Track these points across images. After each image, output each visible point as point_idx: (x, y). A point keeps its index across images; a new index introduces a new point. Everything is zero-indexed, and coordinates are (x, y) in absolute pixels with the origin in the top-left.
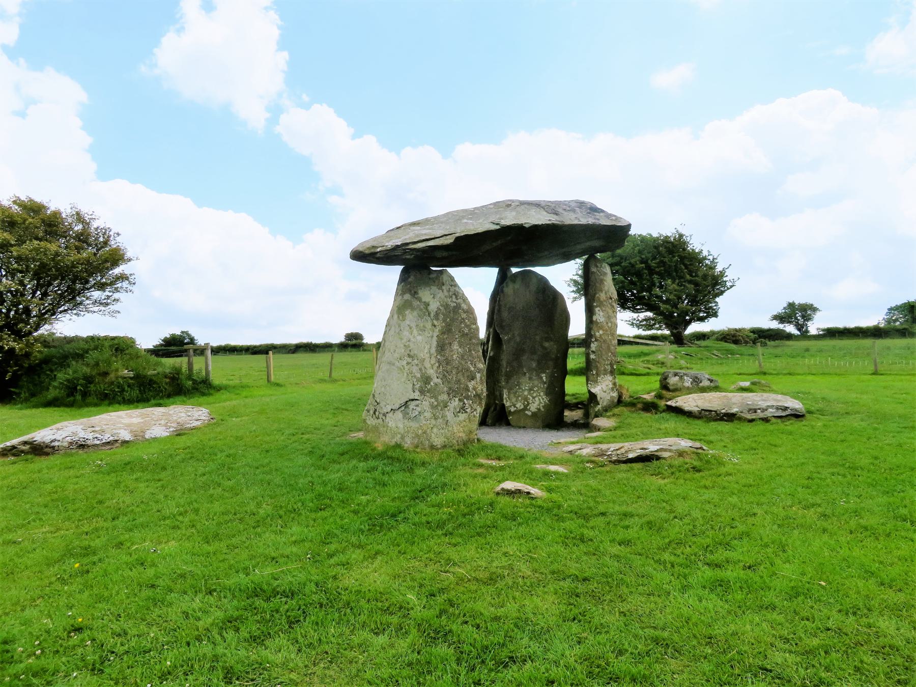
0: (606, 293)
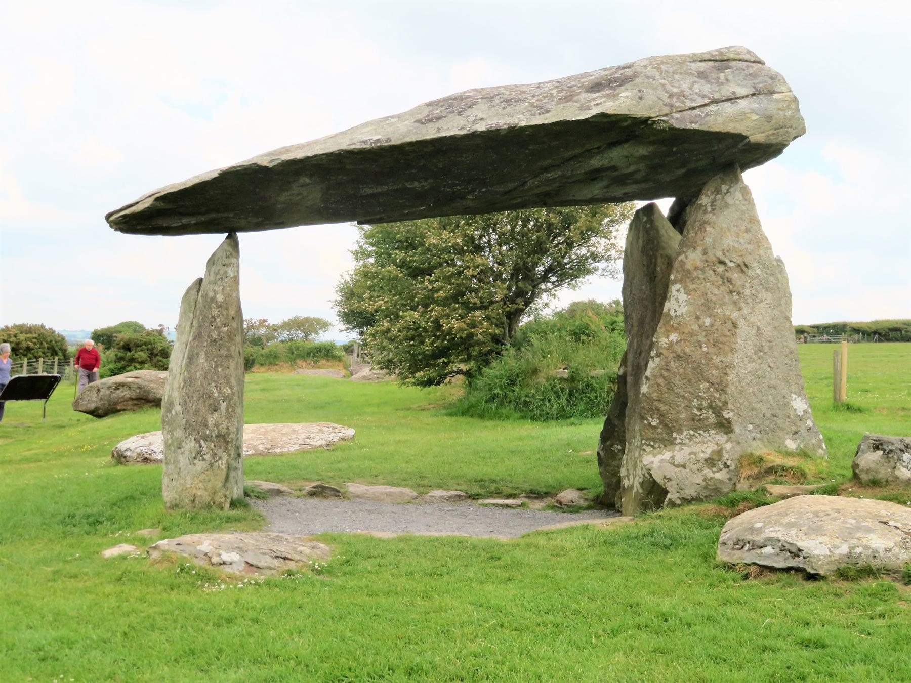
0: (705, 253)
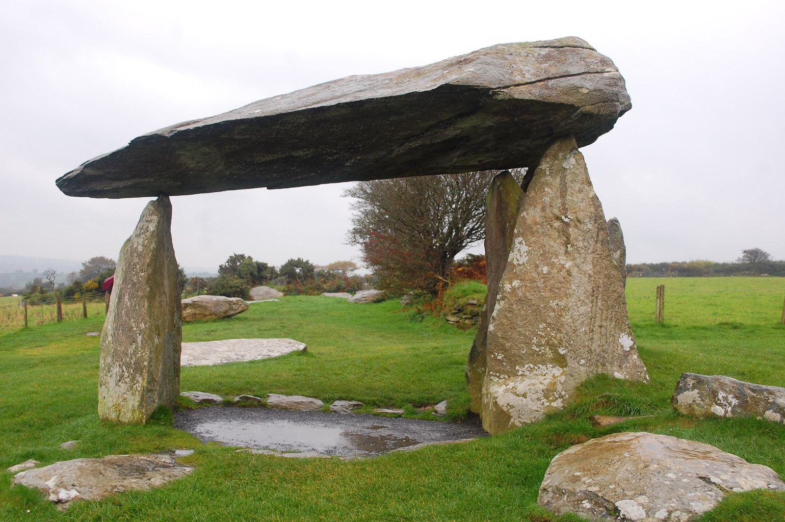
0: (543, 209)
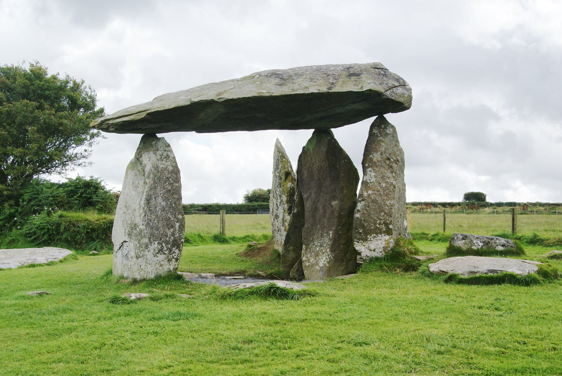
0: (382, 154)
